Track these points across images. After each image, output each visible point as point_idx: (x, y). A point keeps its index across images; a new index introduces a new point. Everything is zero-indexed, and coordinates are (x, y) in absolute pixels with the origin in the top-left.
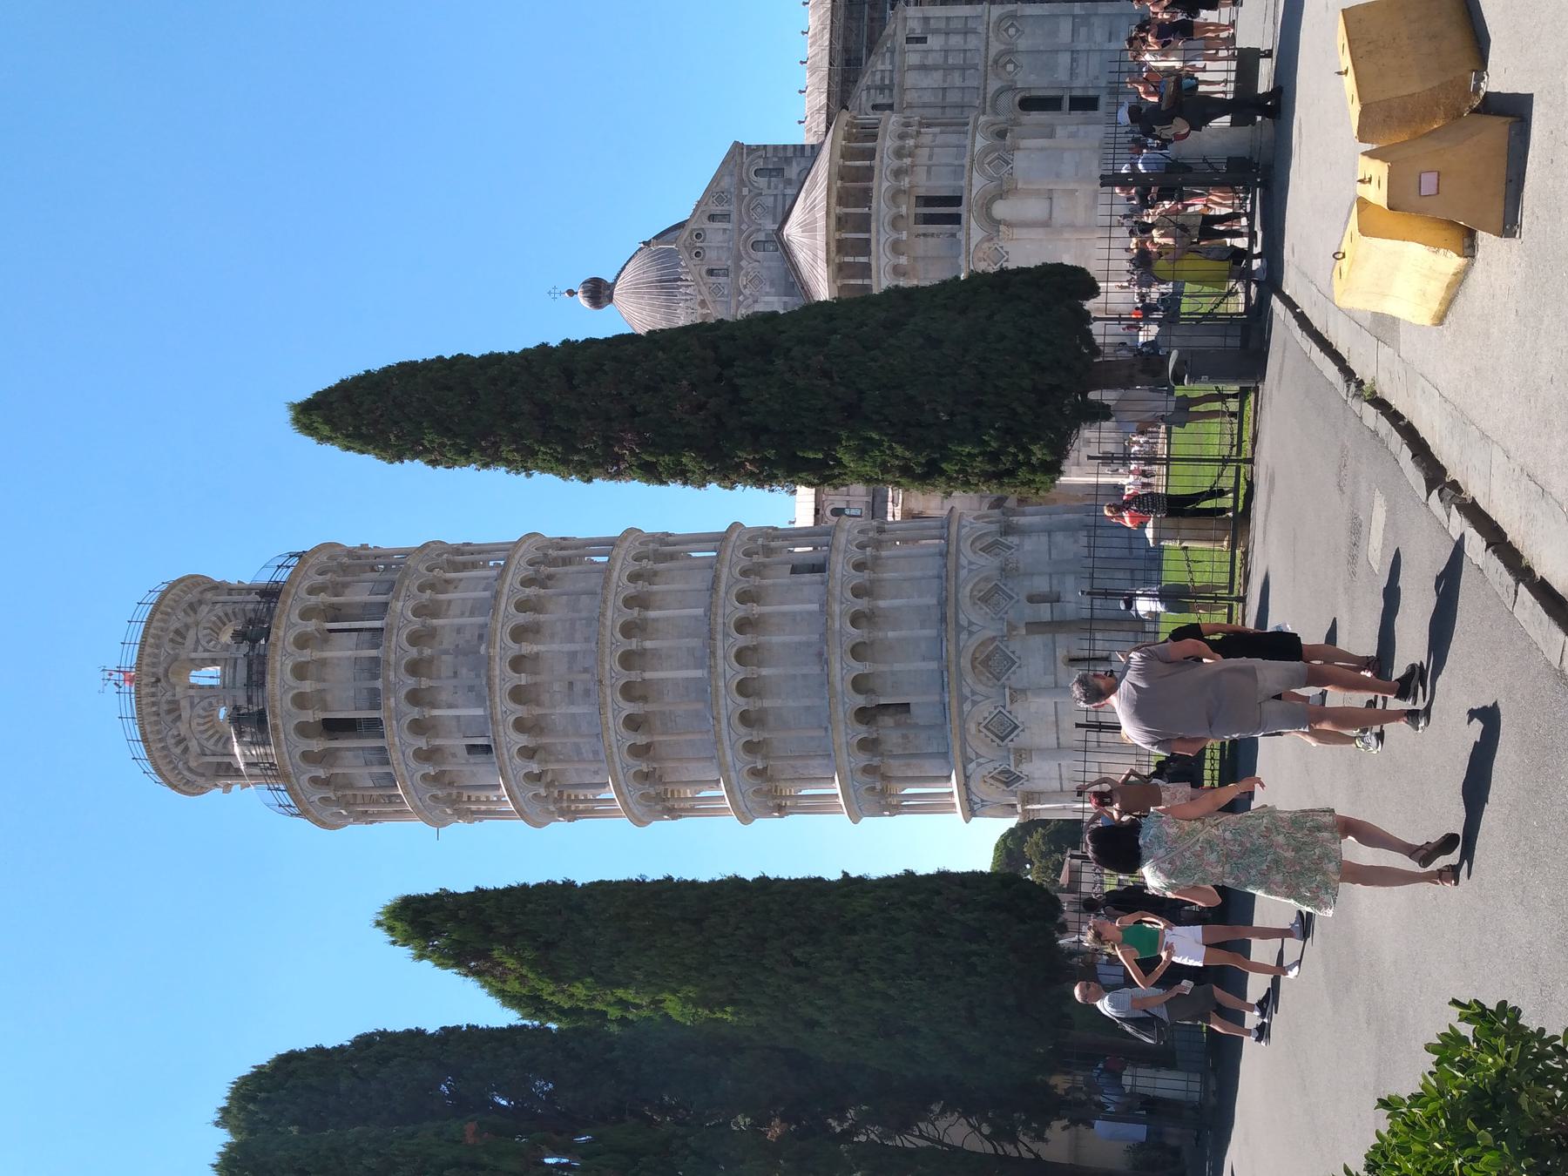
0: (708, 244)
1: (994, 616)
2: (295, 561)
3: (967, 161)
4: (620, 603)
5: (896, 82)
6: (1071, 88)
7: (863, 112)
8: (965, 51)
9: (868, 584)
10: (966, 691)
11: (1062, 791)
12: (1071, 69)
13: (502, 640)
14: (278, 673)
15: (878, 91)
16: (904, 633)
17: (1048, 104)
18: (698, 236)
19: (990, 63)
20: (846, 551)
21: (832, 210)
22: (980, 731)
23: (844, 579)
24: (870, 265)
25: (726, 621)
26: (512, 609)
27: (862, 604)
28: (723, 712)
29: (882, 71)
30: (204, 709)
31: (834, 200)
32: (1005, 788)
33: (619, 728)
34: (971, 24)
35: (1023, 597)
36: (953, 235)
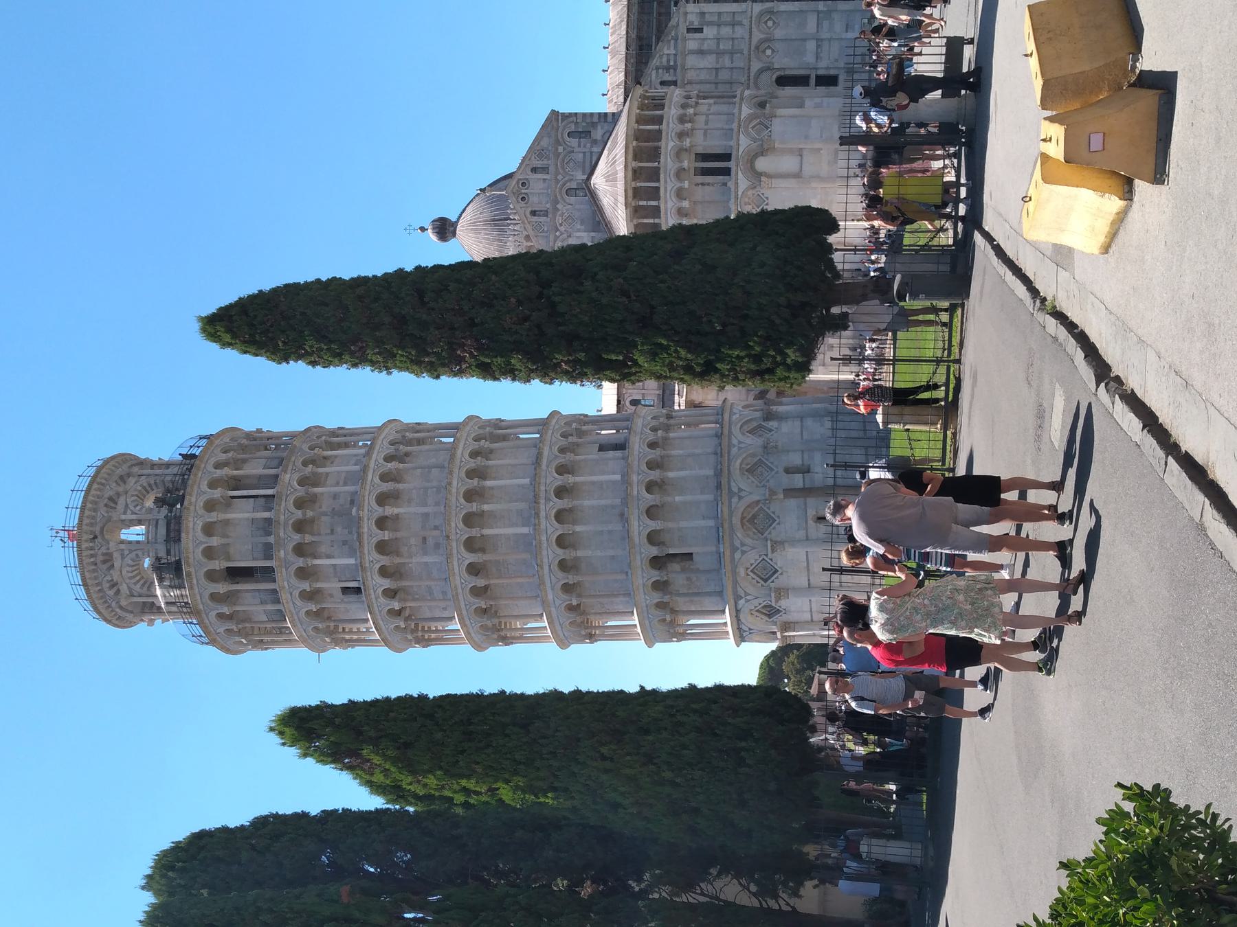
0: (532, 191)
1: (758, 484)
2: (204, 442)
3: (735, 126)
4: (463, 475)
6: (816, 69)
7: (653, 87)
8: (733, 39)
9: (659, 459)
10: (737, 543)
11: (812, 621)
12: (817, 53)
14: (191, 531)
16: (688, 498)
17: (799, 81)
18: (524, 184)
20: (642, 433)
21: (629, 164)
22: (748, 575)
23: (640, 455)
24: (660, 207)
25: (548, 489)
26: (377, 480)
27: (655, 475)
28: (545, 560)
29: (668, 54)
30: (133, 560)
31: (630, 156)
32: (768, 619)
33: (463, 574)
34: (738, 18)
35: (781, 470)
36: (725, 184)
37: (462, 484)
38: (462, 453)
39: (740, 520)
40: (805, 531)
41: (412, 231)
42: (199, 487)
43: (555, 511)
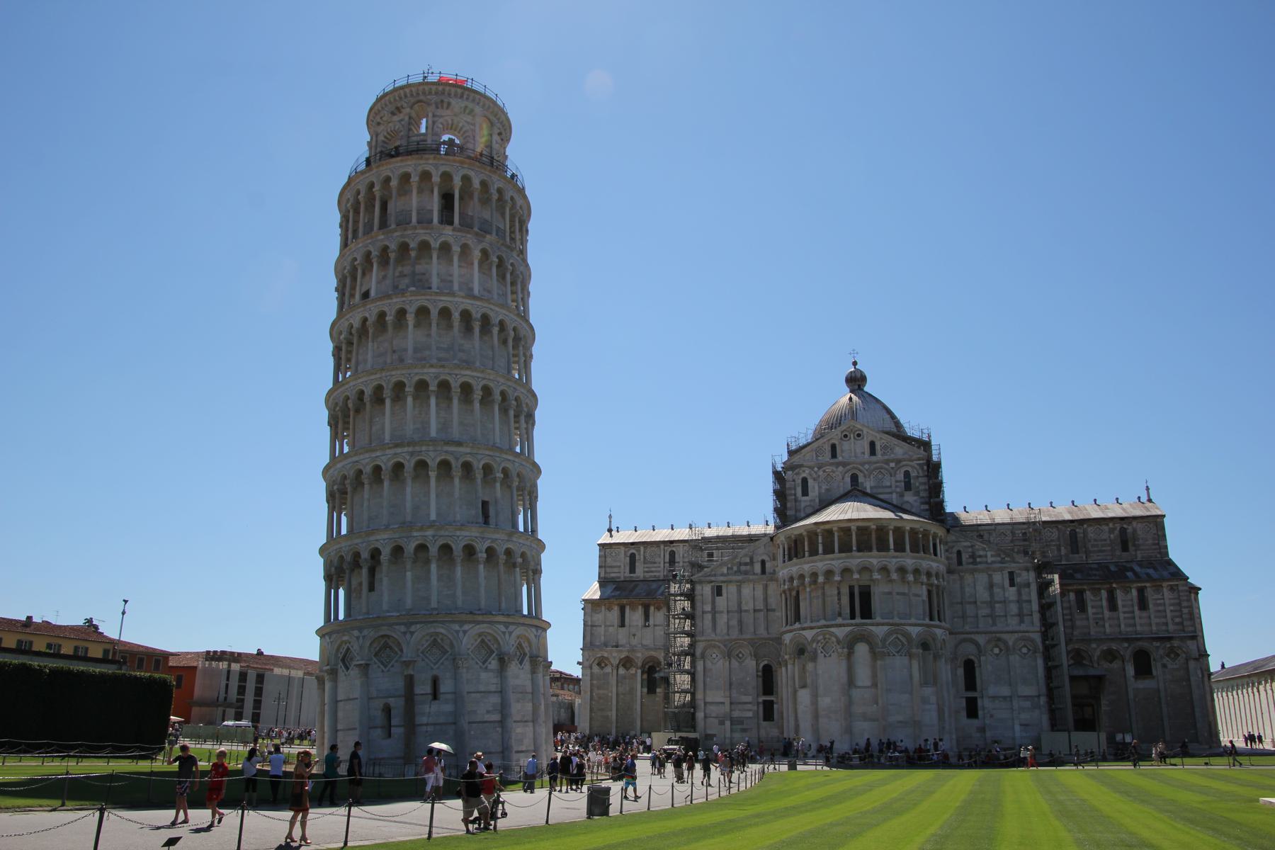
3: (897, 620)
4: (443, 377)
5: (979, 566)
6: (982, 697)
8: (1006, 616)
10: (365, 632)
12: (1000, 697)
13: (417, 300)
15: (970, 554)
17: (970, 682)
19: (998, 635)
20: (483, 538)
21: (853, 524)
25: (423, 453)
27: (433, 550)
28: (362, 457)
29: (986, 556)
34: (1027, 619)
35: (435, 672)
36: (840, 615)
41: (855, 355)
43: (402, 461)
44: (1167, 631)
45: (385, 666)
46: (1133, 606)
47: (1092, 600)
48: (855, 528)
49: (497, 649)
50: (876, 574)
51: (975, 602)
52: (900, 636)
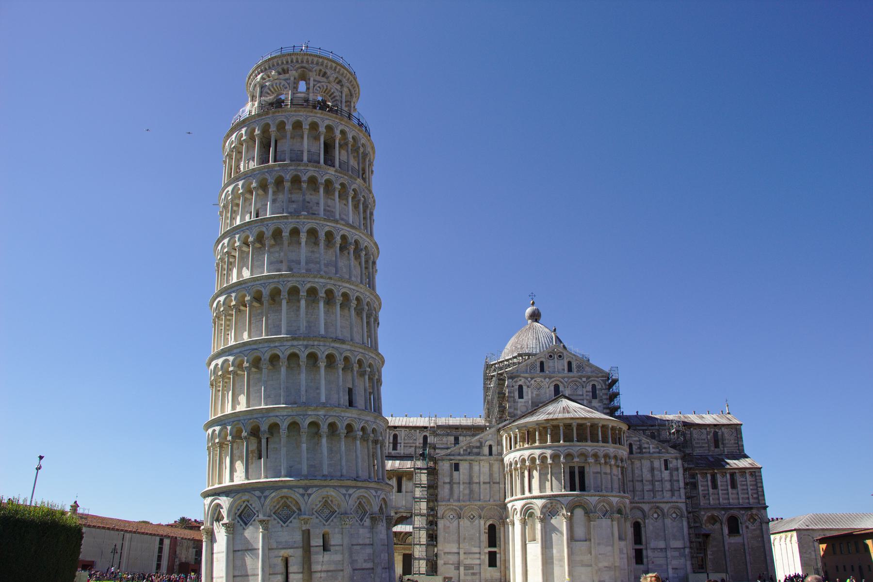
0: (556, 362)
1: (315, 510)
4: (329, 287)
6: (646, 549)
7: (628, 439)
8: (662, 491)
9: (338, 432)
10: (267, 493)
14: (297, 114)
15: (639, 446)
19: (657, 504)
20: (360, 419)
21: (574, 421)
22: (244, 502)
23: (341, 417)
25: (315, 347)
26: (327, 229)
27: (324, 428)
29: (649, 448)
31: (580, 421)
33: (255, 287)
34: (676, 493)
35: (327, 529)
37: (321, 286)
38: (345, 287)
39: (285, 495)
40: (275, 547)
41: (531, 297)
42: (327, 119)
43: (297, 352)
44: (749, 503)
45: (284, 523)
46: (727, 486)
47: (701, 481)
48: (576, 424)
49: (369, 510)
50: (590, 458)
51: (642, 481)
52: (605, 504)
